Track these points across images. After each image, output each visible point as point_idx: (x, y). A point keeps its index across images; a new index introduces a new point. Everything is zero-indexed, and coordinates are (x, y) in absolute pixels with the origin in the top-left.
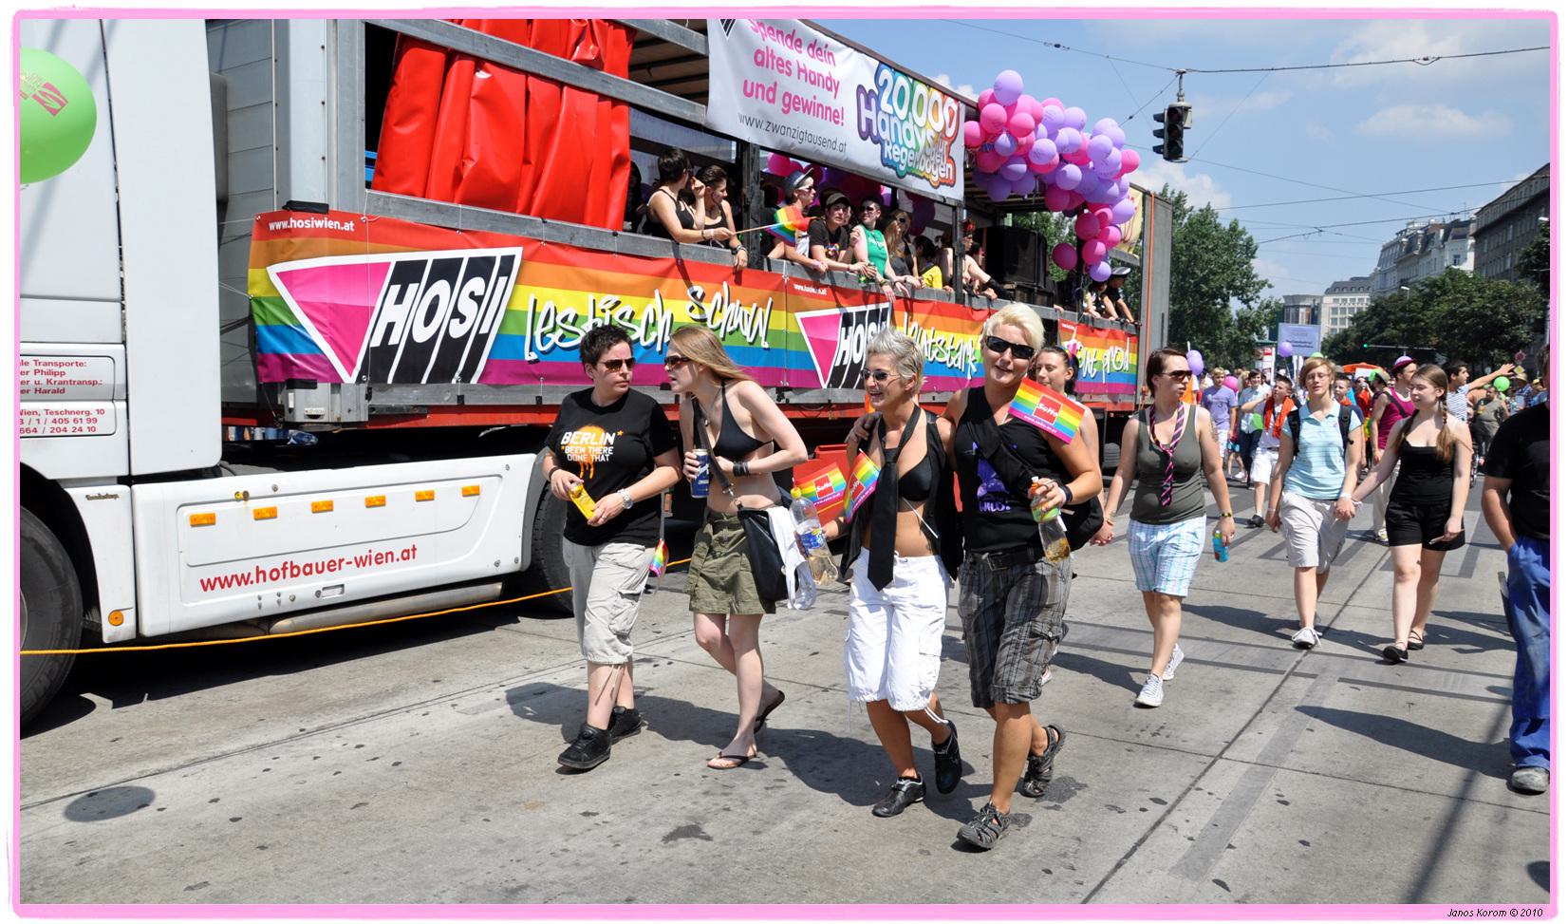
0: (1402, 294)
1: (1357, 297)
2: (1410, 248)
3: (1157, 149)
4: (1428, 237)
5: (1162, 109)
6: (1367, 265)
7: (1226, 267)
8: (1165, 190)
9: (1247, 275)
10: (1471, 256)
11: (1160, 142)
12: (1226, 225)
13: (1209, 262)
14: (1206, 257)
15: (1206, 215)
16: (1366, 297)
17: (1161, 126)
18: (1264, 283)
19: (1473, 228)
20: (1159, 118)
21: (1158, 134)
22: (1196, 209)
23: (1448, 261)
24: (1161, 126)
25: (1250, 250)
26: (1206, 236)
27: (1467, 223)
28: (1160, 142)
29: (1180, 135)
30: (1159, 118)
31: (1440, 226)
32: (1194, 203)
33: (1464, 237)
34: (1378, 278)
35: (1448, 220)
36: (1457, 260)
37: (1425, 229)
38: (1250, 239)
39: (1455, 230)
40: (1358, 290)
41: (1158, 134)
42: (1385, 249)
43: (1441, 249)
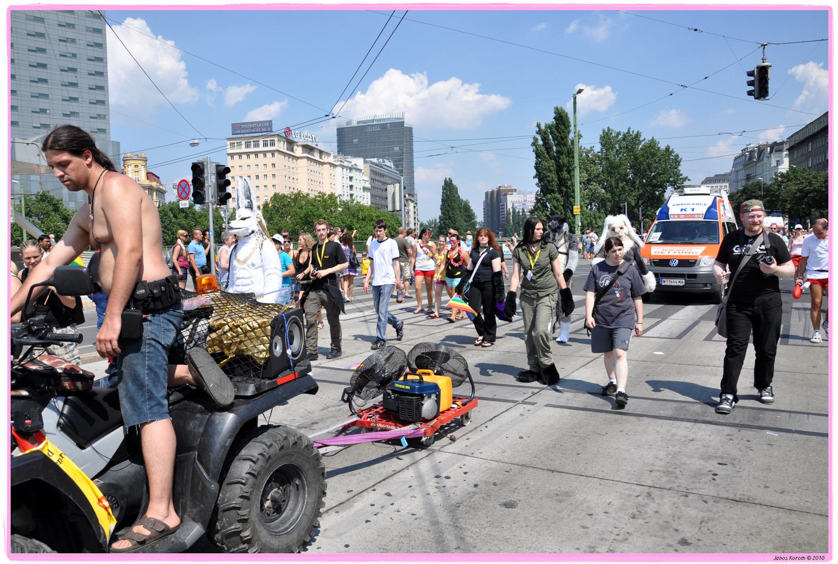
0: (759, 183)
1: (723, 185)
2: (751, 158)
3: (750, 93)
4: (761, 150)
5: (753, 67)
6: (726, 167)
7: (665, 171)
8: (629, 131)
9: (678, 175)
10: (786, 161)
11: (752, 88)
12: (662, 146)
13: (656, 168)
14: (655, 165)
15: (652, 144)
16: (727, 184)
17: (752, 78)
18: (686, 178)
19: (786, 147)
20: (750, 74)
21: (750, 83)
22: (647, 141)
23: (774, 164)
24: (752, 78)
25: (677, 161)
26: (653, 155)
27: (782, 143)
28: (752, 88)
29: (767, 82)
30: (750, 74)
31: (767, 145)
32: (646, 137)
33: (781, 151)
34: (734, 174)
35: (770, 142)
36: (778, 163)
37: (759, 147)
38: (677, 156)
39: (776, 147)
40: (724, 181)
41: (750, 83)
42: (736, 159)
43: (769, 158)
